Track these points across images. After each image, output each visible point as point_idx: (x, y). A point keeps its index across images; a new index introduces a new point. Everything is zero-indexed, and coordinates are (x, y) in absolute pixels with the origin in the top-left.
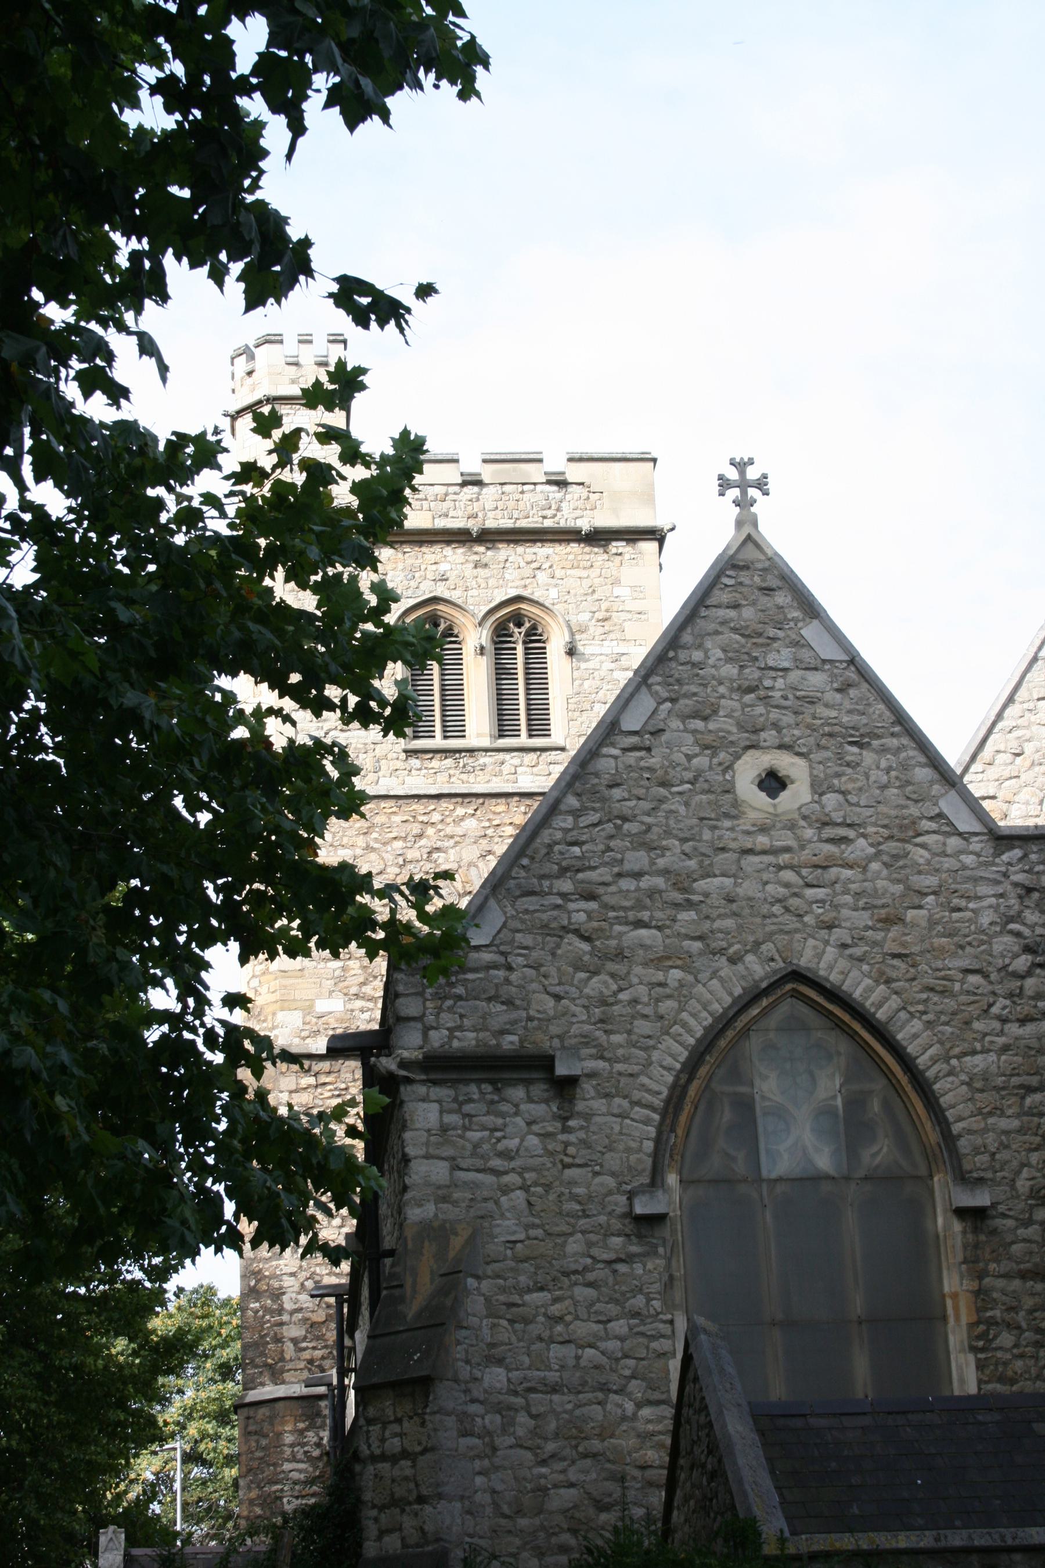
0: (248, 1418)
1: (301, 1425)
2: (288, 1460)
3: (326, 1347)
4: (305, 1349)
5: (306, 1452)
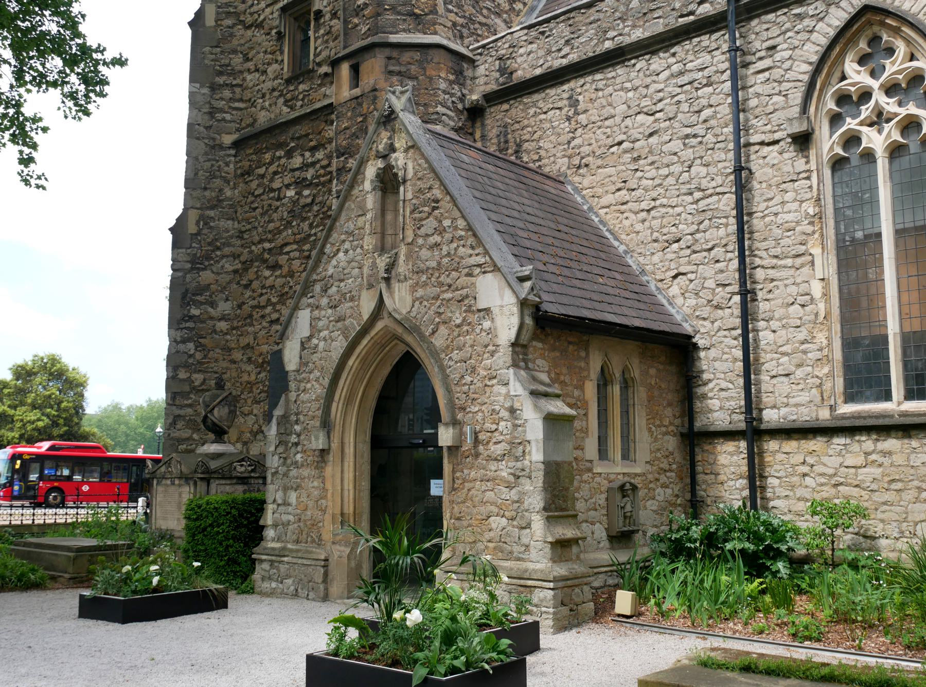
0: (389, 58)
1: (452, 77)
2: (441, 104)
3: (464, 17)
4: (451, 11)
5: (453, 102)
